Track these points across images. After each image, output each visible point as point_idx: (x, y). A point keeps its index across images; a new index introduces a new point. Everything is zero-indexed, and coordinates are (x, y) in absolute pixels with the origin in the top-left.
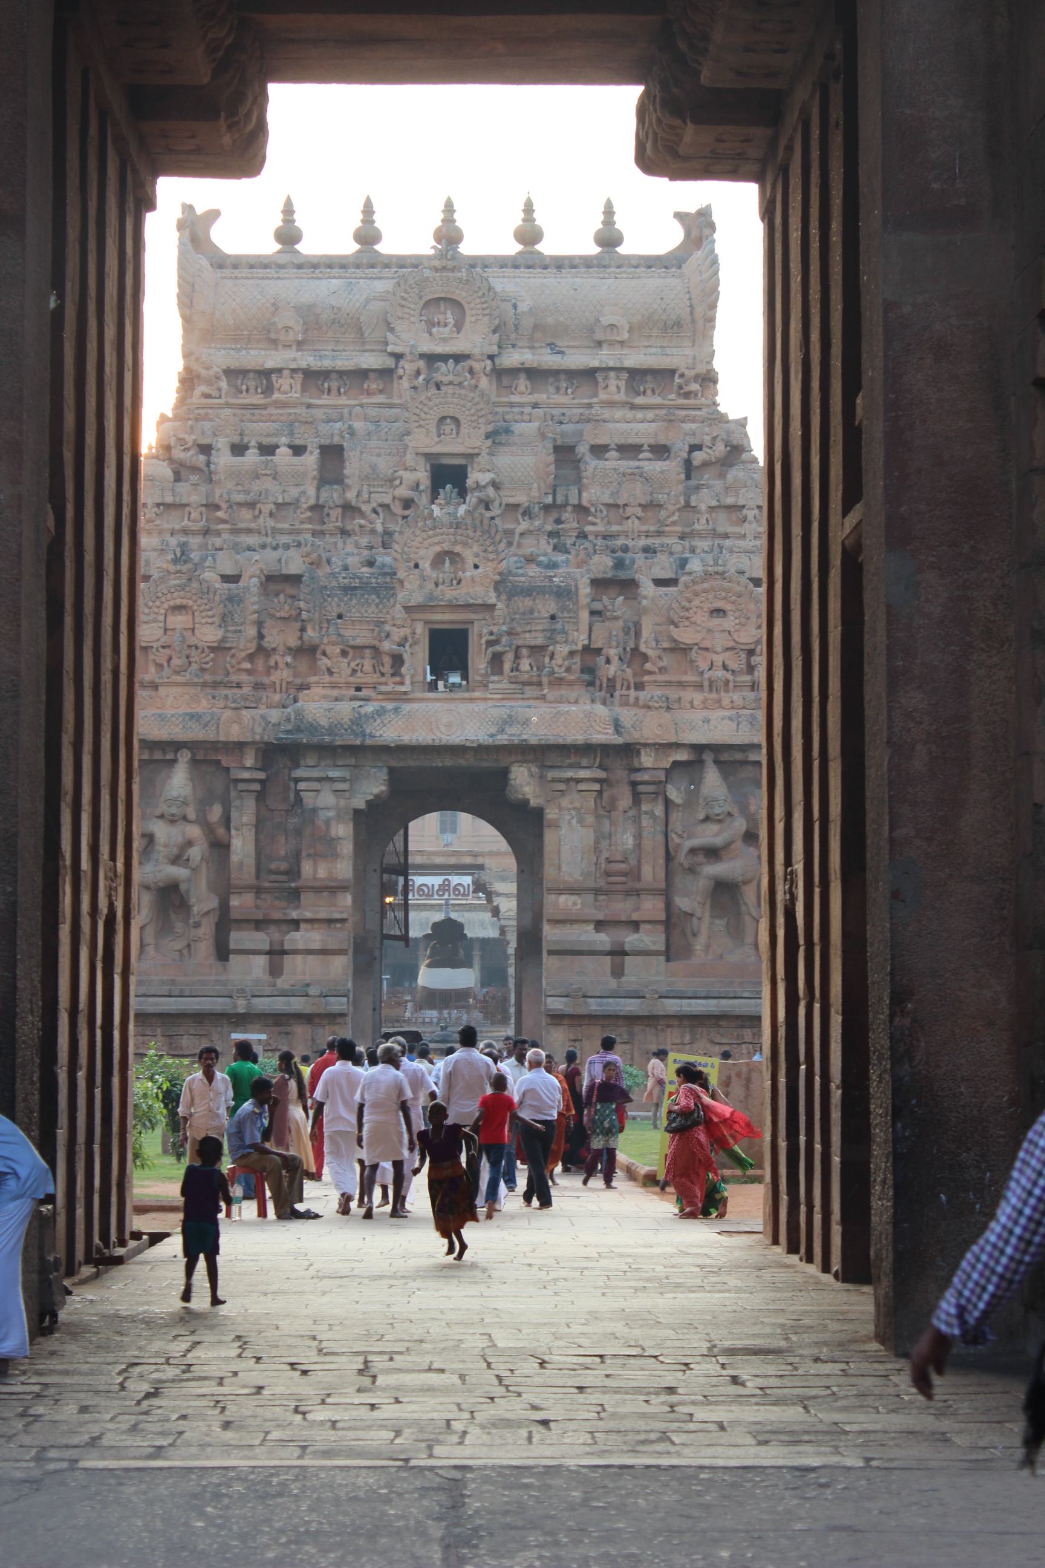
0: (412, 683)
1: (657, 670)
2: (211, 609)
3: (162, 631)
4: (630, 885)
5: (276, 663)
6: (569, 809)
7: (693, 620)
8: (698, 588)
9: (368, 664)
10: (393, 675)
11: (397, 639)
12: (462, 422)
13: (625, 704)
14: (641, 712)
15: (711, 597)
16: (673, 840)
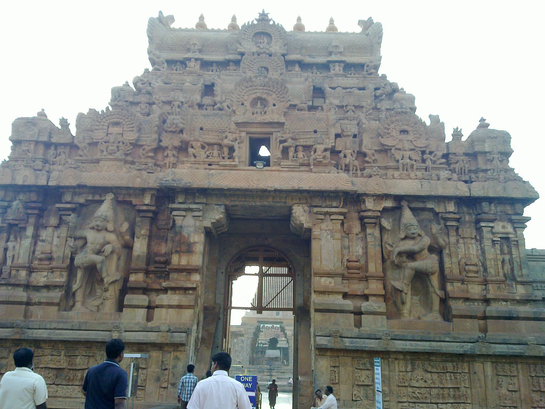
0: (239, 162)
1: (372, 161)
2: (133, 123)
3: (105, 134)
4: (362, 274)
5: (168, 154)
6: (326, 230)
7: (392, 134)
8: (394, 119)
9: (216, 153)
10: (229, 158)
11: (231, 138)
12: (269, 69)
13: (356, 176)
14: (366, 179)
15: (400, 124)
16: (386, 248)
